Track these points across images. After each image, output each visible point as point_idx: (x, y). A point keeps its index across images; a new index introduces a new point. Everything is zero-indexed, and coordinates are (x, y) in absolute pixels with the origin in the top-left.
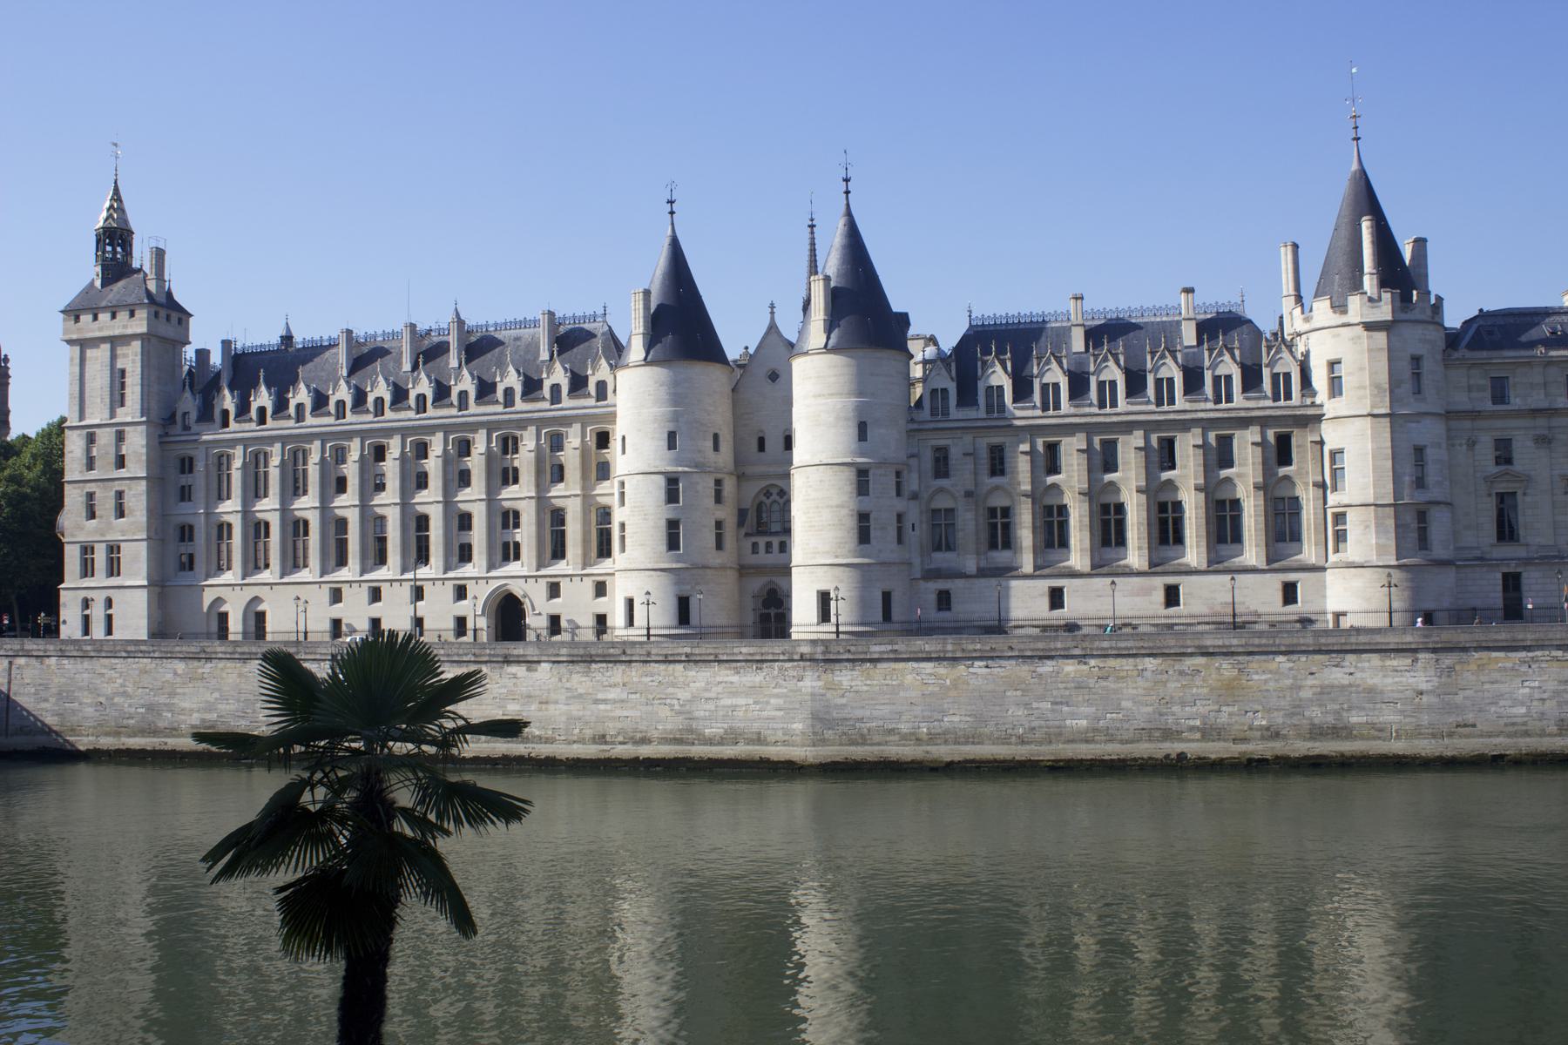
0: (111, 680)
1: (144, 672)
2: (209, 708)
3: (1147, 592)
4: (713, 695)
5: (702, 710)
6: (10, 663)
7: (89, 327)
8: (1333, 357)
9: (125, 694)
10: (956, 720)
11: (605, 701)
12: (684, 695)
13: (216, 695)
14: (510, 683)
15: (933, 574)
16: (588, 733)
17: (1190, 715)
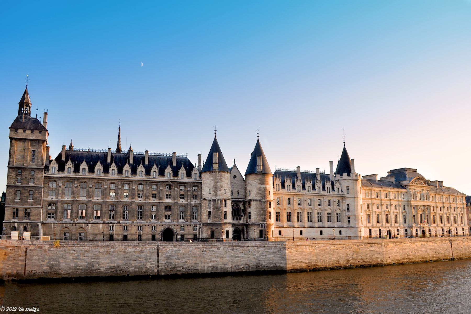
0: (72, 254)
3: (317, 232)
4: (264, 255)
5: (262, 258)
7: (21, 134)
8: (347, 185)
11: (238, 257)
13: (116, 258)
15: (278, 227)
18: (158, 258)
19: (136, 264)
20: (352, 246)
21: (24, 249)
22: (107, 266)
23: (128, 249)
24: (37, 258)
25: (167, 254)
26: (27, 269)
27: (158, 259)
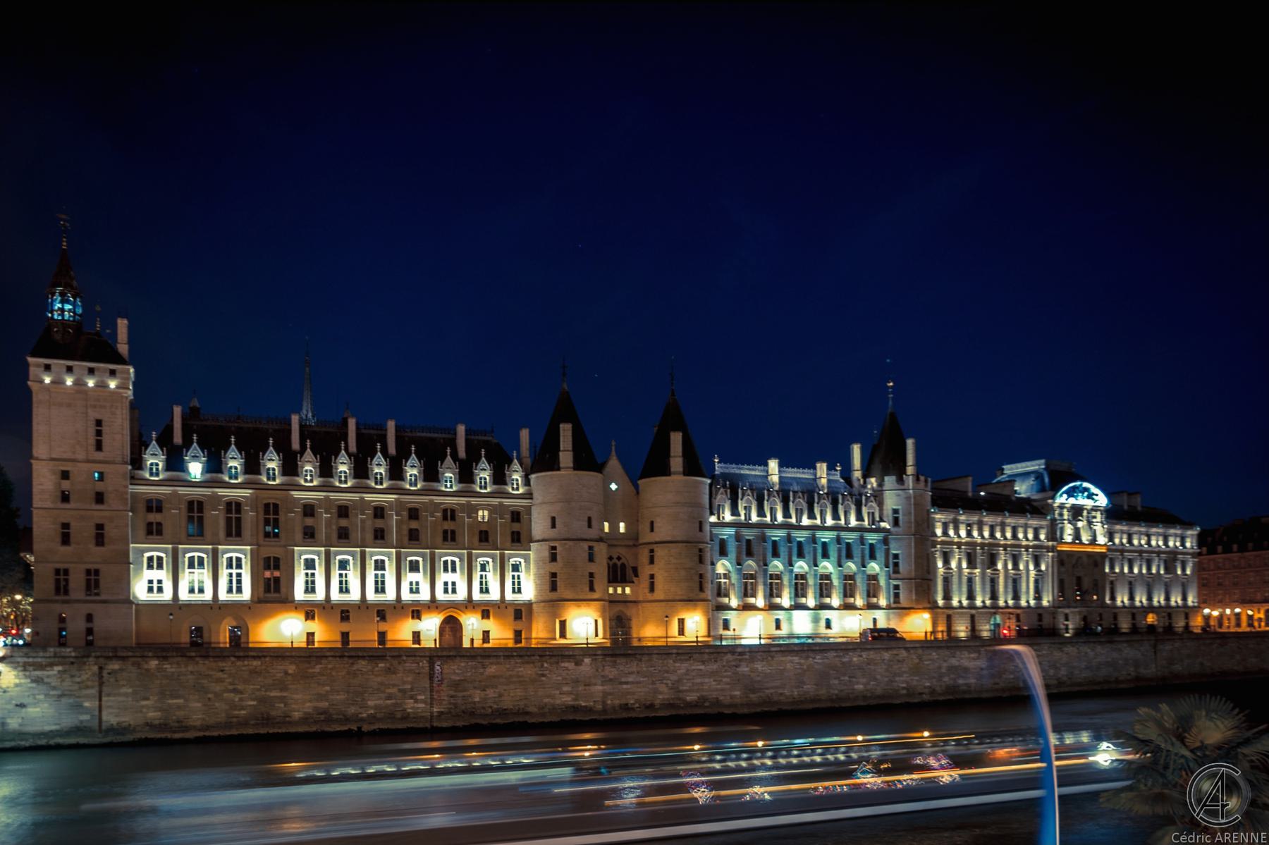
1: (254, 672)
2: (321, 697)
6: (101, 668)
9: (235, 691)
10: (809, 688)
11: (627, 683)
12: (674, 678)
13: (328, 688)
14: (564, 674)
16: (617, 702)
17: (901, 682)
18: (431, 686)
19: (378, 702)
20: (904, 653)
21: (95, 668)
22: (308, 707)
23: (355, 667)
24: (130, 690)
25: (453, 677)
26: (104, 718)
27: (431, 691)
